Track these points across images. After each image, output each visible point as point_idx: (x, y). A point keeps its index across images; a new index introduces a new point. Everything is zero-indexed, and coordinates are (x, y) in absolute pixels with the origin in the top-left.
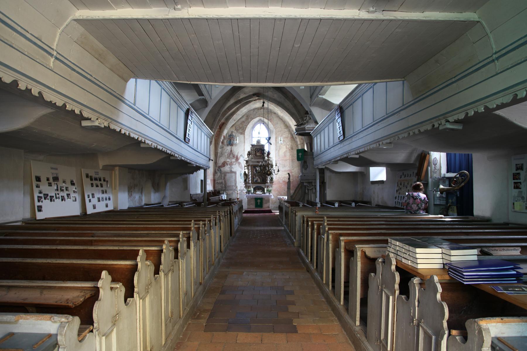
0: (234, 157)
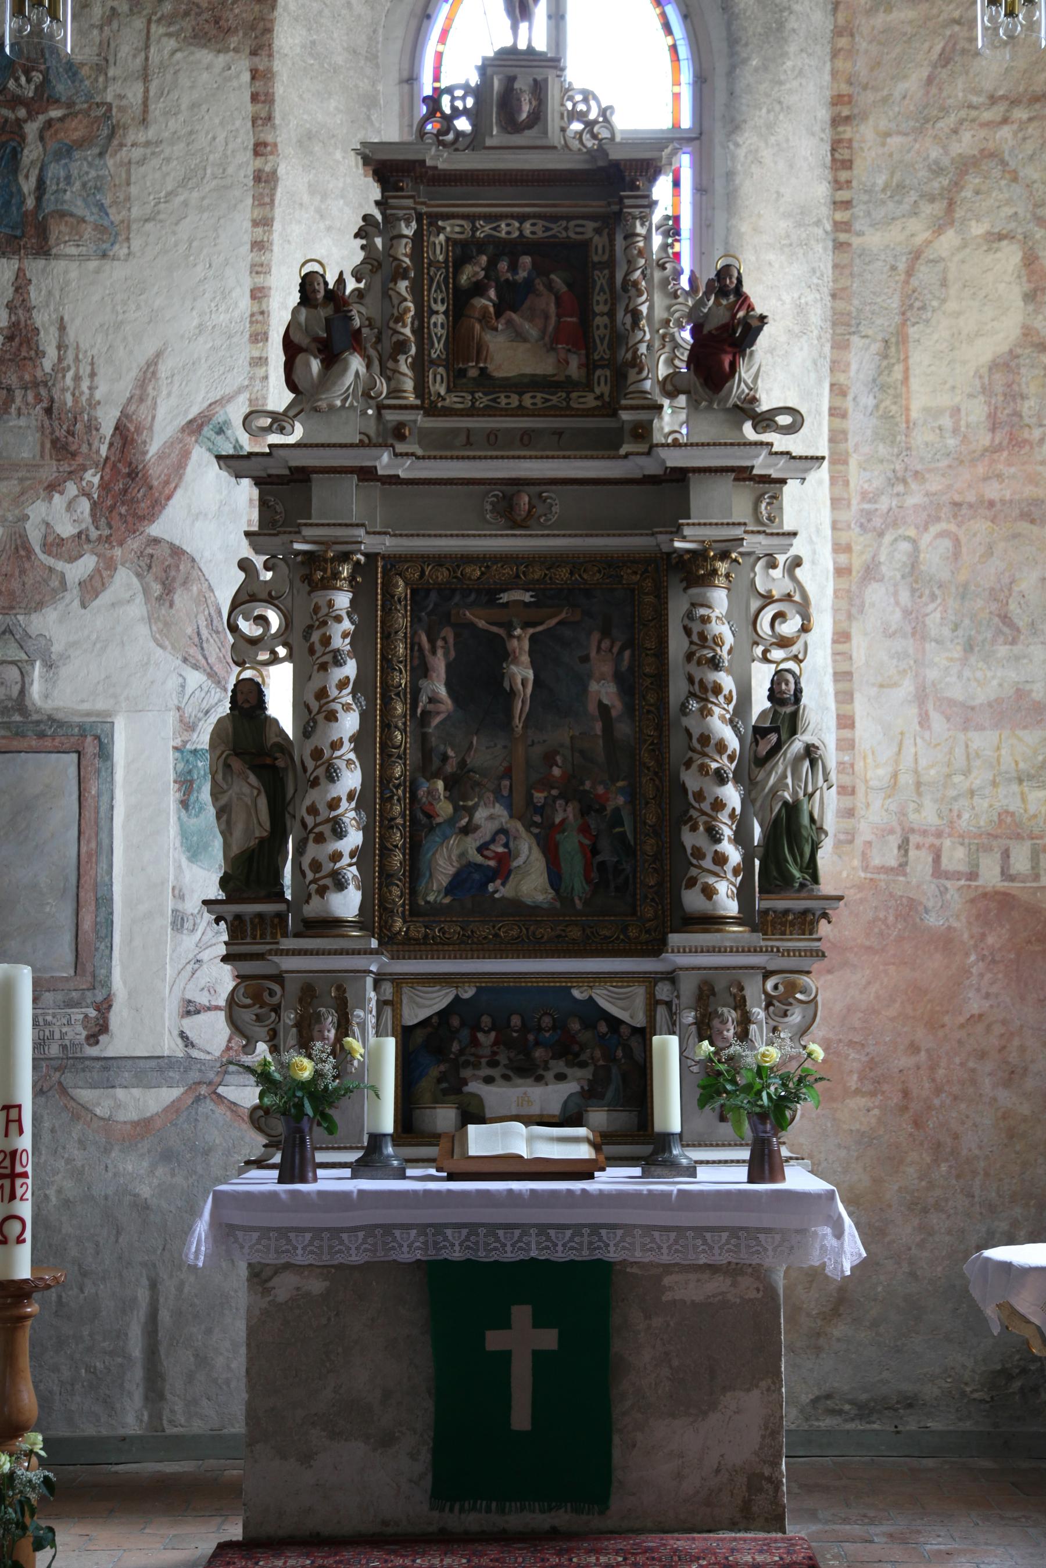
0: (64, 444)
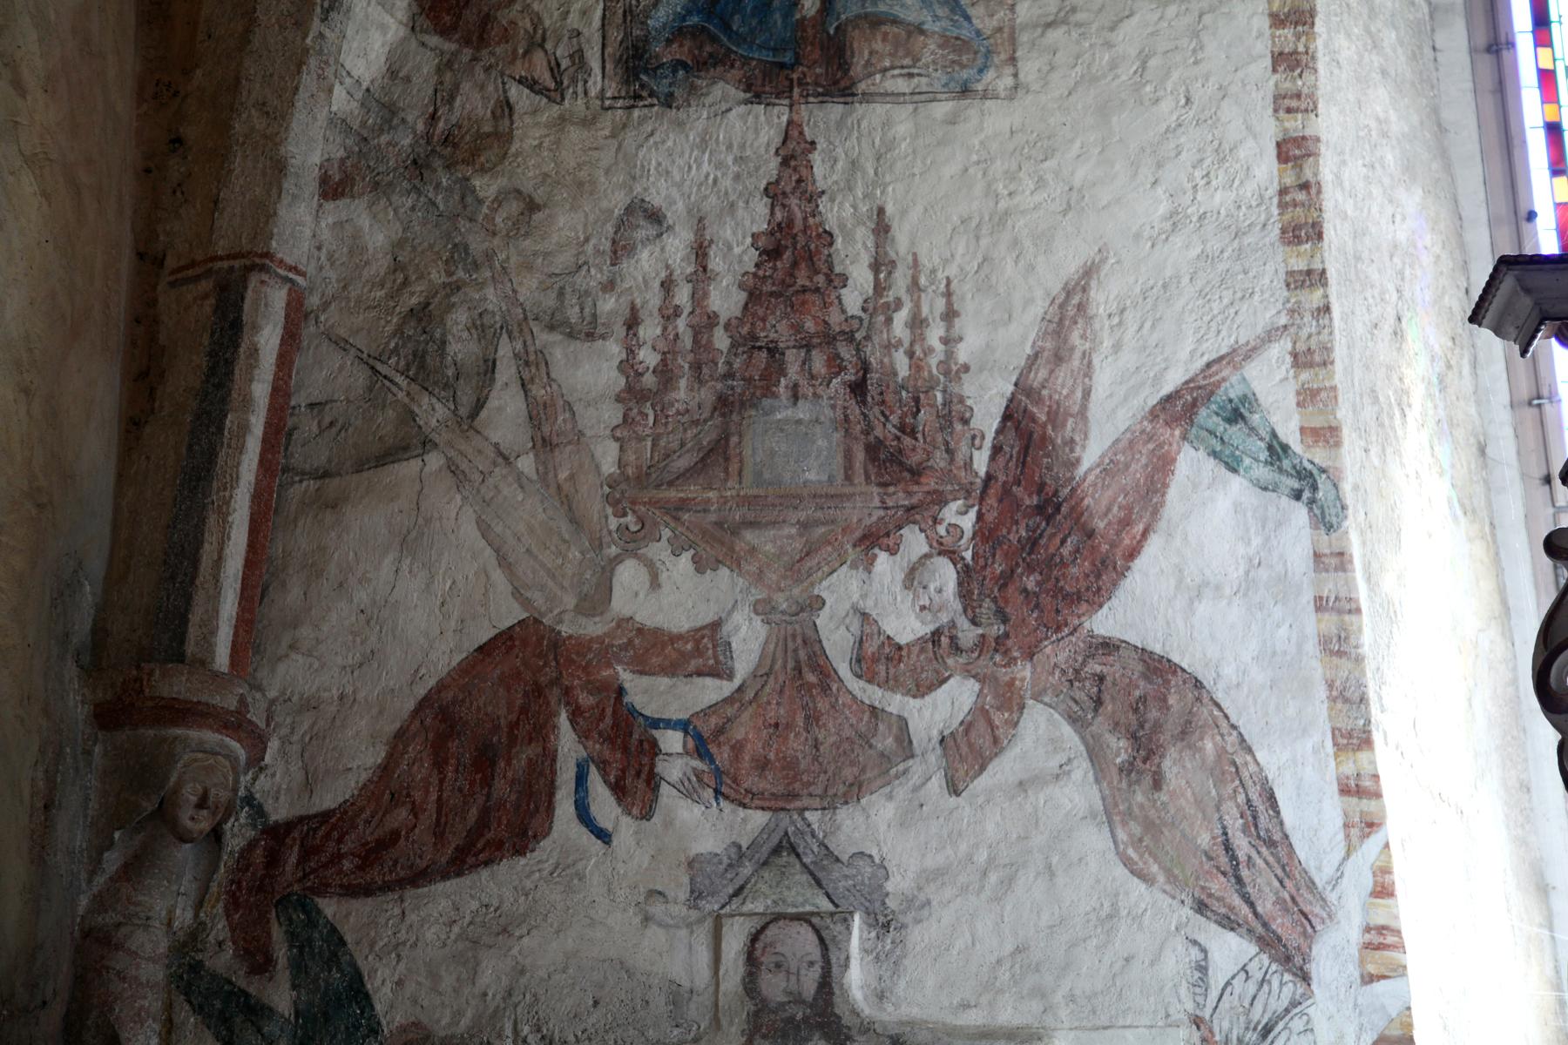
0: (894, 446)
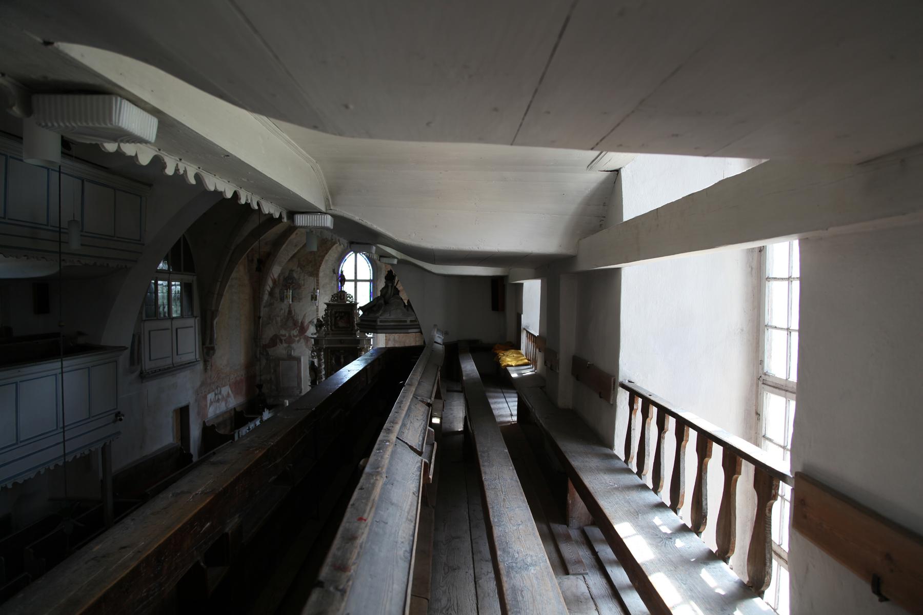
0: (295, 323)
